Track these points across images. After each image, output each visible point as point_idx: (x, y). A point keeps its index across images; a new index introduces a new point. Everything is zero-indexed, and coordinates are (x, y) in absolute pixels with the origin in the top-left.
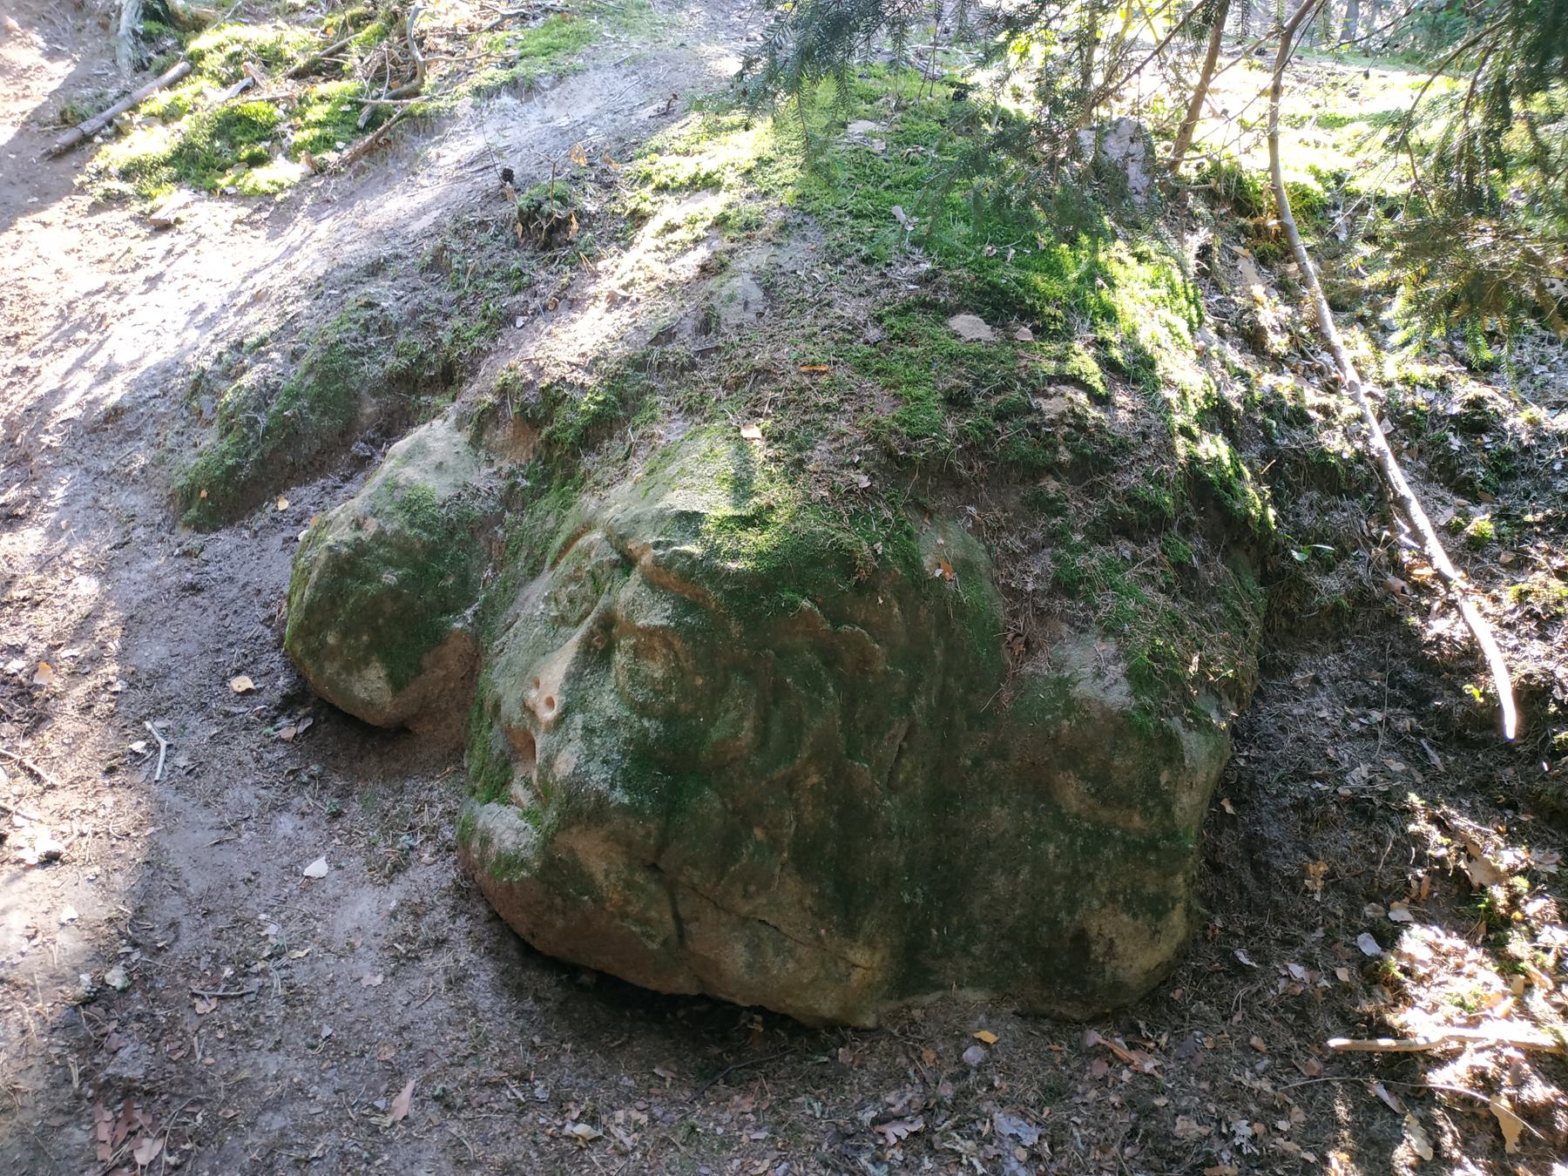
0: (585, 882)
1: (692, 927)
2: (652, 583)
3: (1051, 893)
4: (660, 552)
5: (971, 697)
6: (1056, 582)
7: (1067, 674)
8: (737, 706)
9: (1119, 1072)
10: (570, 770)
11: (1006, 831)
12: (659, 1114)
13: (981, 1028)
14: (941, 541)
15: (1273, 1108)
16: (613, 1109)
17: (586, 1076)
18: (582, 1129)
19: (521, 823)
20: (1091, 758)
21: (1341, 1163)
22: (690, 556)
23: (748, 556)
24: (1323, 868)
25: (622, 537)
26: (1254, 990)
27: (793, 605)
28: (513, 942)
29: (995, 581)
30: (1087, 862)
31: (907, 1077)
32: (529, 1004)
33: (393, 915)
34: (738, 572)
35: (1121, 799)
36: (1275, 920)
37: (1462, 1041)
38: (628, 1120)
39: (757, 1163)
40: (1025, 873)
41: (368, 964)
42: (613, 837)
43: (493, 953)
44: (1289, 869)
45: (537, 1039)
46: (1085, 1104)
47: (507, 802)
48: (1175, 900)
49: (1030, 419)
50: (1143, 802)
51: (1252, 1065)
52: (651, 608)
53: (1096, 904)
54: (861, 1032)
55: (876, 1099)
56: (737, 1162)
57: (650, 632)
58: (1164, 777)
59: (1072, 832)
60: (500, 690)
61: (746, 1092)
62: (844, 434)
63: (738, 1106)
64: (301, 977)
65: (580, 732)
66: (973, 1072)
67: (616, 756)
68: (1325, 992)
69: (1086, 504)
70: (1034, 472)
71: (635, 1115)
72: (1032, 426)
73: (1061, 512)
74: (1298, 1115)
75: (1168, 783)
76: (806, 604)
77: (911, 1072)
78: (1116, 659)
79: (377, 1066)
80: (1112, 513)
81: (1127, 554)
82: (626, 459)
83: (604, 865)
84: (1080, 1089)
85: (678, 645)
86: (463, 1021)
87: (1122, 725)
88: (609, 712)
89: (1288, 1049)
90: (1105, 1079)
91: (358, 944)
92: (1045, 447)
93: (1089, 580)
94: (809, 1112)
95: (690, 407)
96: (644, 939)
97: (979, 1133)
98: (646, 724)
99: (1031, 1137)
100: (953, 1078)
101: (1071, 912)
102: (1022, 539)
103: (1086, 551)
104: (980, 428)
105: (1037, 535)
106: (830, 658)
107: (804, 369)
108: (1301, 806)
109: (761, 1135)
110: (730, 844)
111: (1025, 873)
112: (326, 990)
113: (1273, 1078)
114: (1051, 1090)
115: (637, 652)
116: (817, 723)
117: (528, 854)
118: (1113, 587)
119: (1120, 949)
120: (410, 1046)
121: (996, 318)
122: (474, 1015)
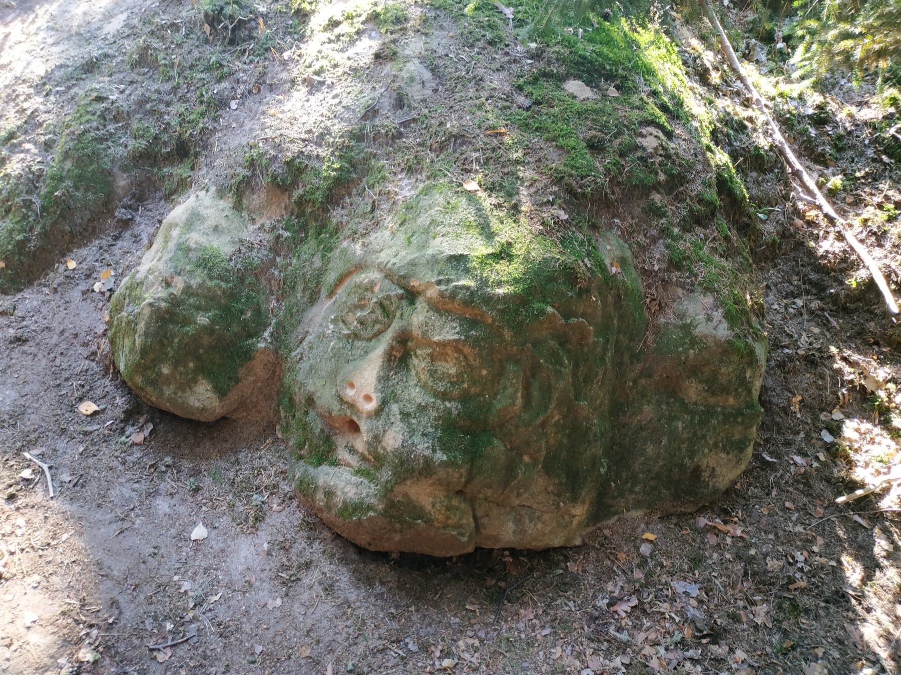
0: (418, 512)
1: (485, 521)
2: (438, 307)
3: (680, 449)
4: (443, 288)
5: (631, 344)
6: (671, 261)
7: (689, 321)
8: (512, 385)
9: (724, 539)
10: (398, 443)
11: (652, 418)
12: (483, 636)
13: (644, 532)
14: (609, 248)
15: (808, 541)
16: (455, 641)
17: (430, 625)
18: (447, 663)
19: (355, 479)
20: (706, 369)
21: (848, 562)
22: (468, 288)
23: (507, 282)
24: (800, 398)
25: (404, 277)
26: (779, 475)
27: (542, 312)
28: (351, 549)
29: (636, 267)
30: (702, 429)
31: (615, 572)
32: (379, 589)
33: (269, 553)
34: (505, 296)
35: (725, 390)
36: (778, 432)
37: (889, 482)
38: (467, 646)
39: (553, 650)
40: (664, 441)
41: (266, 592)
42: (440, 482)
43: (344, 561)
44: (782, 402)
45: (393, 610)
46: (714, 563)
47: (335, 463)
48: (750, 440)
49: (639, 154)
50: (736, 390)
51: (790, 518)
52: (442, 328)
53: (706, 451)
54: (578, 549)
55: (601, 590)
56: (541, 653)
57: (444, 344)
58: (748, 375)
59: (692, 413)
60: (311, 388)
61: (524, 605)
62: (535, 181)
63: (525, 616)
64: (223, 615)
65: (398, 417)
66: (649, 560)
67: (430, 430)
68: (817, 470)
69: (676, 207)
70: (646, 190)
71: (470, 641)
72: (640, 158)
73: (663, 215)
74: (820, 541)
75: (750, 377)
76: (550, 309)
77: (615, 568)
78: (716, 307)
79: (303, 662)
80: (691, 211)
81: (702, 236)
82: (373, 210)
83: (431, 499)
84: (707, 554)
85: (467, 350)
86: (345, 613)
87: (727, 349)
88: (418, 401)
89: (805, 505)
90: (718, 545)
91: (253, 580)
92: (651, 172)
93: (688, 257)
94: (567, 608)
95: (410, 167)
96: (459, 537)
97: (667, 596)
98: (448, 405)
99: (694, 591)
100: (639, 566)
101: (691, 458)
102: (645, 235)
103: (682, 238)
104: (615, 164)
105: (654, 232)
106: (563, 340)
107: (488, 132)
108: (781, 365)
109: (547, 631)
110: (510, 470)
111: (664, 441)
112: (244, 620)
113: (802, 523)
114: (694, 559)
115: (433, 358)
116: (561, 385)
117: (373, 501)
118: (701, 260)
119: (718, 472)
120: (318, 642)
121: (591, 82)
122: (349, 607)
